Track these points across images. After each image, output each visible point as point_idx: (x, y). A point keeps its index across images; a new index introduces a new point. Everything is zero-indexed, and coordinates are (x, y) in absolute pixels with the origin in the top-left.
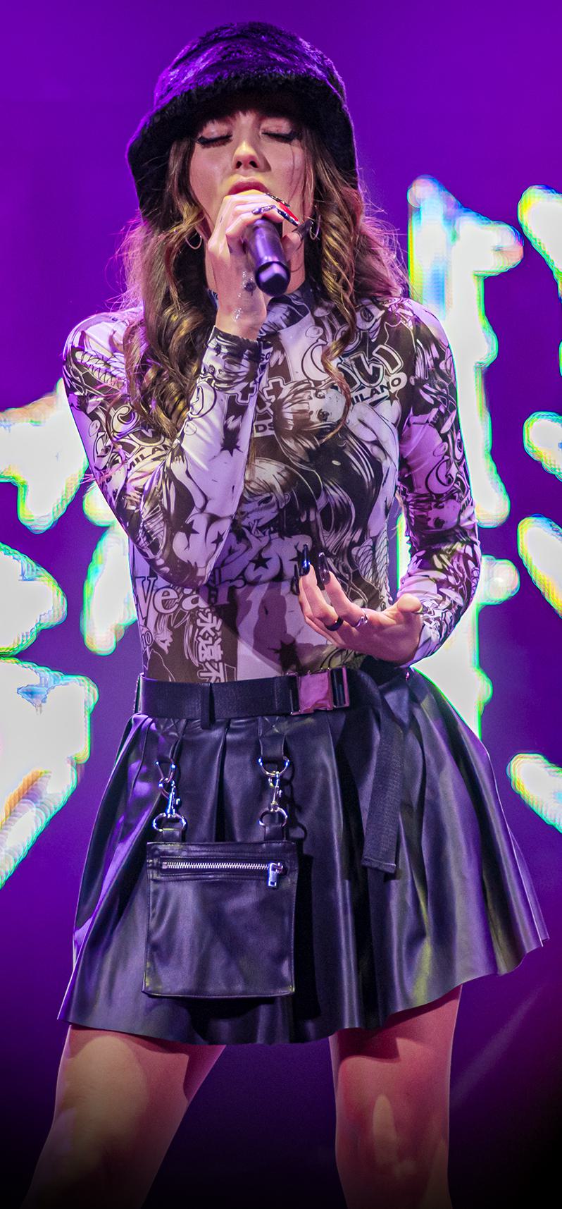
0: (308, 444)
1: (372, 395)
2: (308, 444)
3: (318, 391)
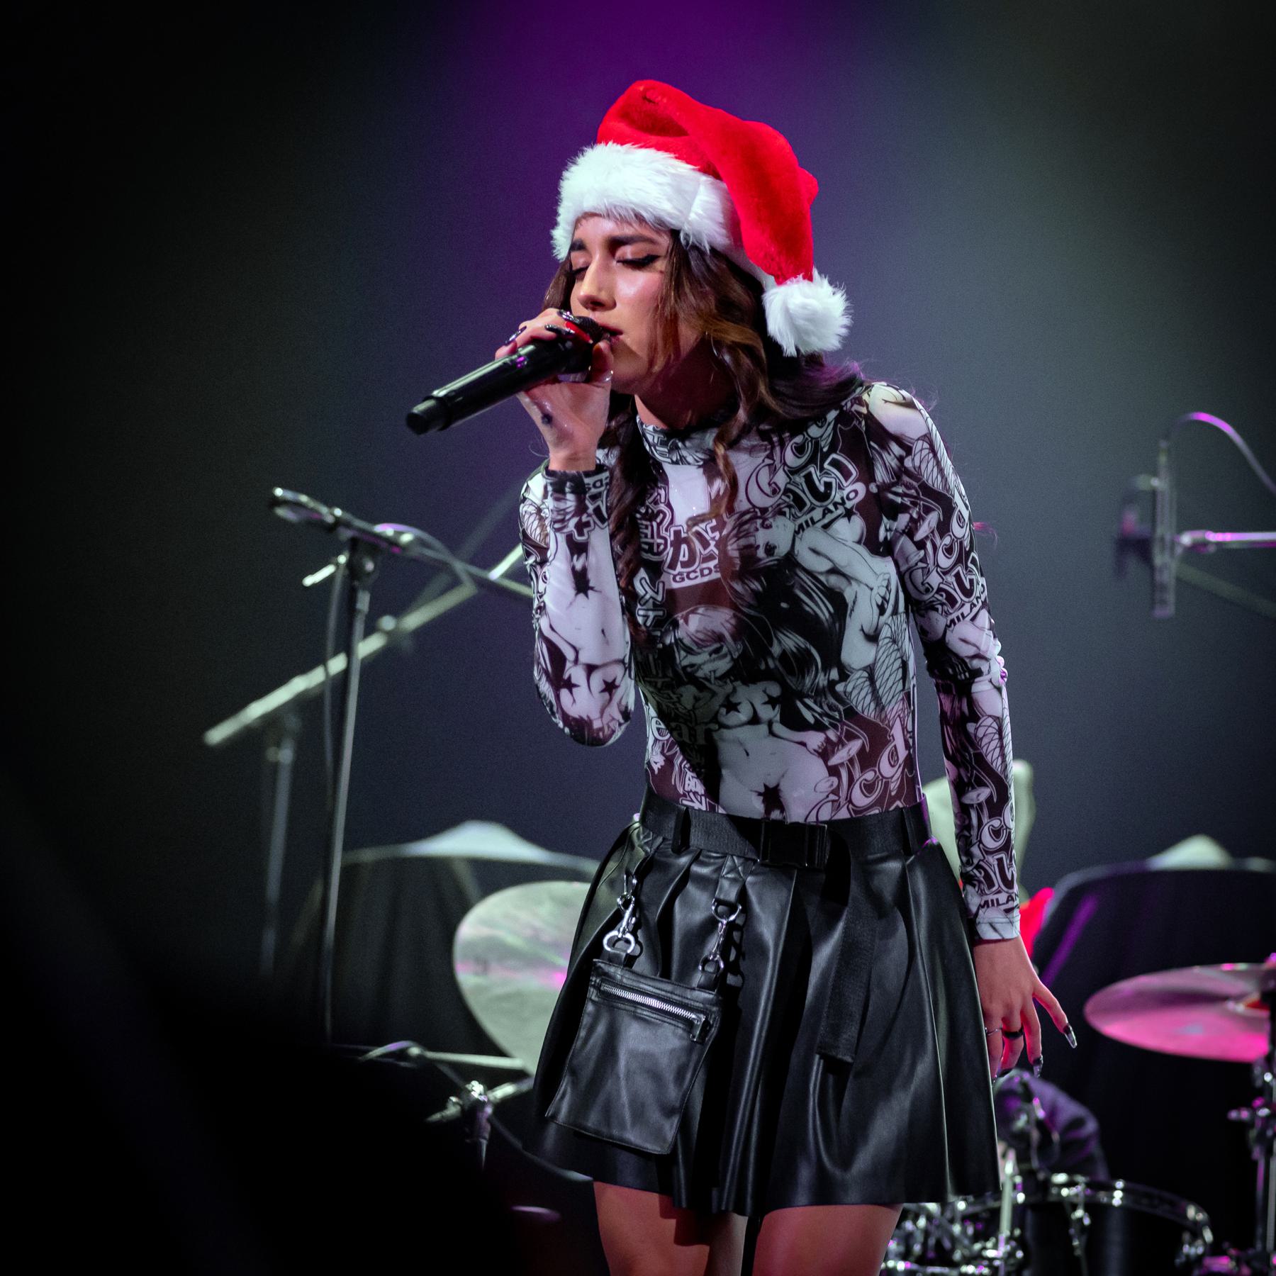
0: (756, 586)
1: (824, 515)
2: (756, 586)
3: (765, 520)
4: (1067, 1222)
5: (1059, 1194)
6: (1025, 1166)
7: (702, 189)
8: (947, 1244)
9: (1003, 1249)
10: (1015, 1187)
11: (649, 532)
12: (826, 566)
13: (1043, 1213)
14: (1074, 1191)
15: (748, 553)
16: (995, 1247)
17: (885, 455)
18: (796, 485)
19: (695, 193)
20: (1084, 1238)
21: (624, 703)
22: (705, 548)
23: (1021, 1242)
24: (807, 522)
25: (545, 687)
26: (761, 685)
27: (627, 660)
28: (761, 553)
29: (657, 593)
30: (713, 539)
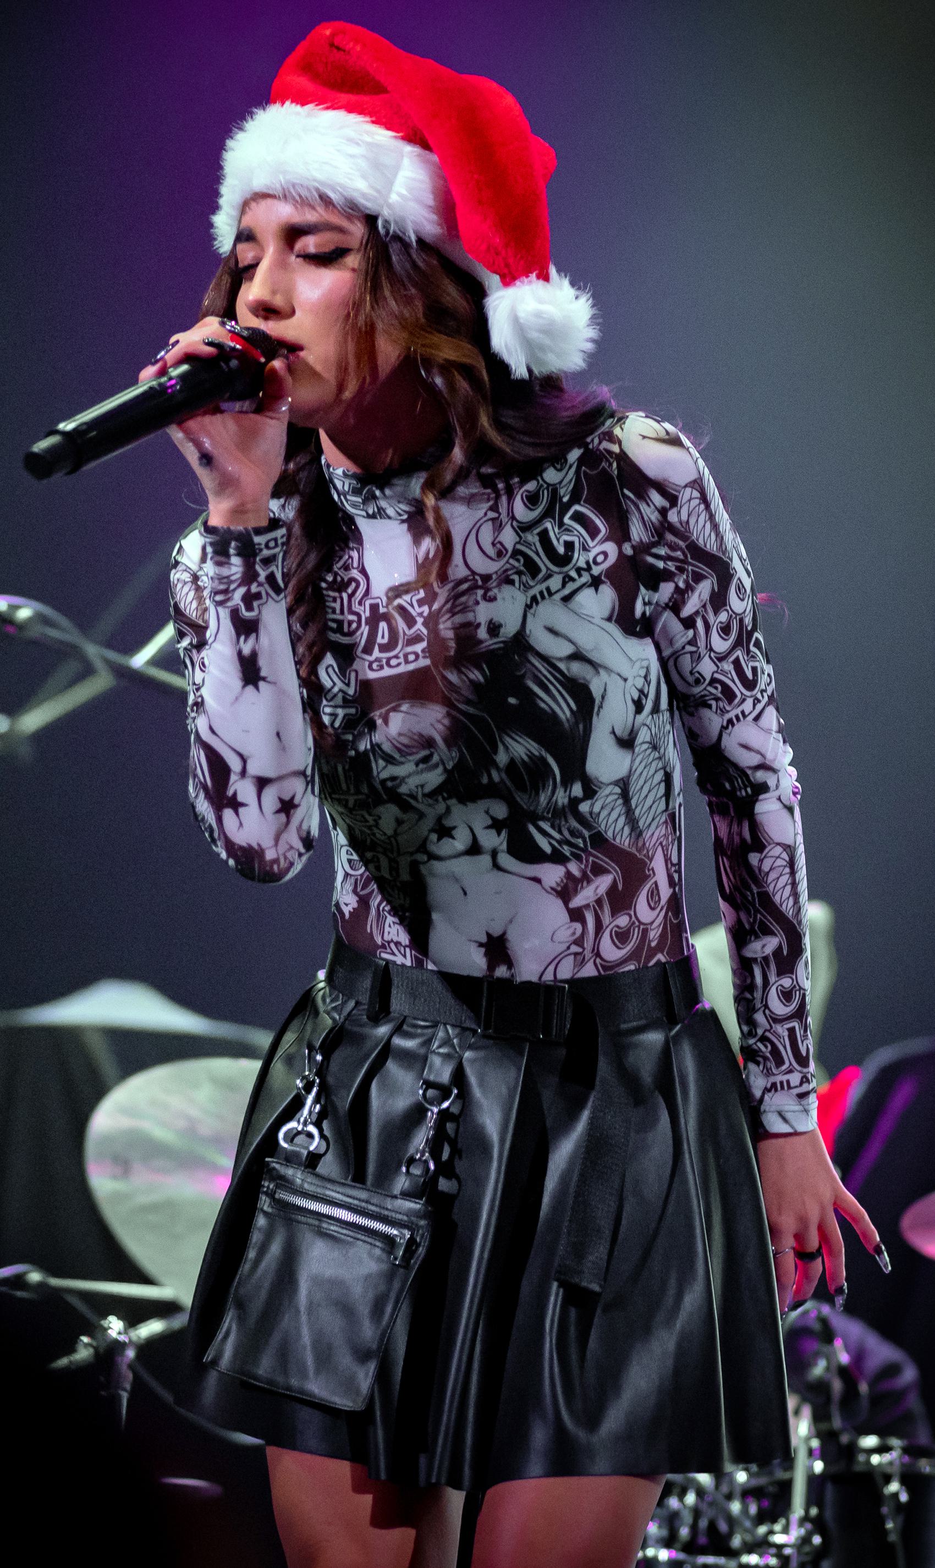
1: (564, 585)
3: (487, 590)
4: (878, 1498)
5: (868, 1462)
6: (824, 1426)
7: (406, 162)
8: (723, 1527)
9: (796, 1533)
10: (811, 1452)
11: (337, 606)
12: (567, 650)
13: (848, 1486)
14: (887, 1457)
15: (465, 634)
16: (786, 1530)
17: (643, 506)
18: (528, 545)
19: (397, 168)
20: (900, 1519)
21: (305, 827)
22: (410, 627)
23: (818, 1525)
24: (541, 593)
25: (203, 807)
26: (482, 804)
27: (309, 772)
28: (482, 633)
29: (348, 685)
30: (421, 614)
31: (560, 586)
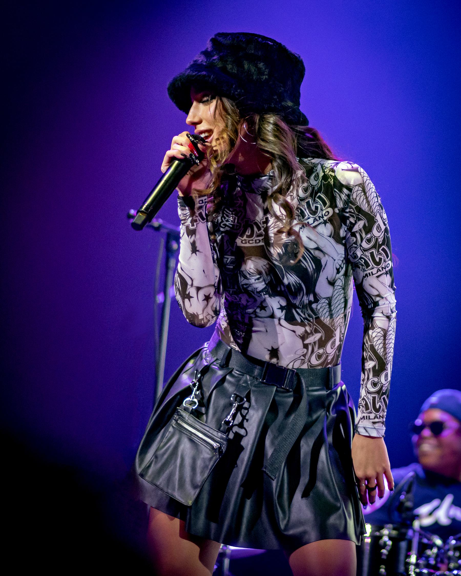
31: (312, 222)
